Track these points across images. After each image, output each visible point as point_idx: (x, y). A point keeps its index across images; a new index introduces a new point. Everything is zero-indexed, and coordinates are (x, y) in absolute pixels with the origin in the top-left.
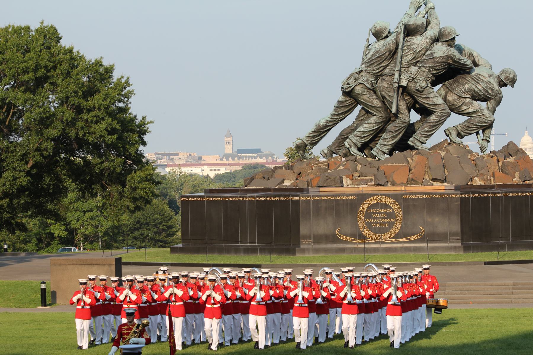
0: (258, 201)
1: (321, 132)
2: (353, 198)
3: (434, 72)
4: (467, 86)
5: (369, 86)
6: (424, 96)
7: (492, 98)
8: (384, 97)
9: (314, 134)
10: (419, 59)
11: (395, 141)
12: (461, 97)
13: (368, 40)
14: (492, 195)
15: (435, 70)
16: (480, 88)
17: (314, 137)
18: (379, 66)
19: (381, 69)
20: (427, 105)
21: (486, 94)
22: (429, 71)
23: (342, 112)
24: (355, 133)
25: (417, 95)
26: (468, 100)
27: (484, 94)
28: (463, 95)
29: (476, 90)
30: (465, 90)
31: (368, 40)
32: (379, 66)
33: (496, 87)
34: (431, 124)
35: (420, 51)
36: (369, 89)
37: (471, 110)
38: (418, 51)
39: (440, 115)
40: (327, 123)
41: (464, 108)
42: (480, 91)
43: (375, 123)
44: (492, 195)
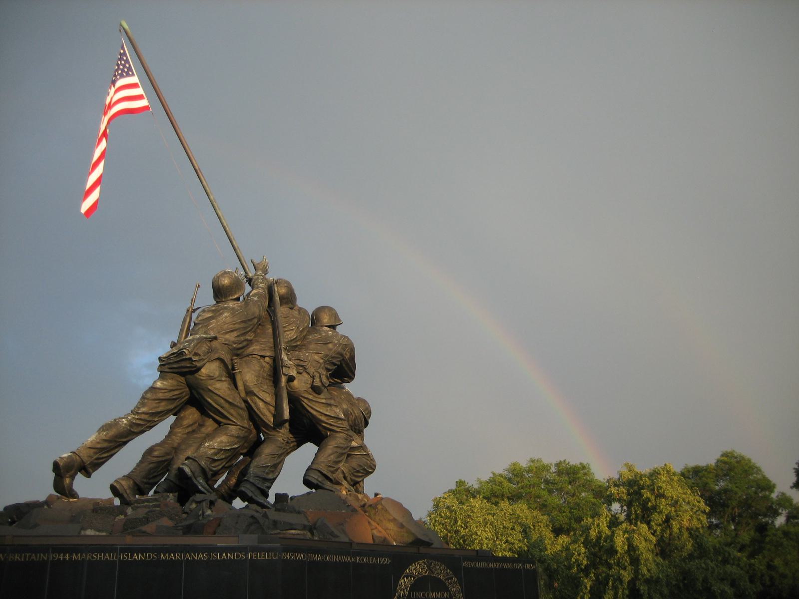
0: (123, 563)
1: (116, 440)
2: (386, 561)
5: (230, 367)
6: (324, 401)
8: (249, 393)
9: (105, 445)
10: (298, 343)
13: (193, 301)
17: (102, 450)
18: (242, 338)
19: (245, 343)
20: (323, 418)
22: (325, 362)
23: (160, 409)
25: (311, 397)
31: (193, 301)
32: (242, 338)
40: (131, 426)
43: (237, 437)
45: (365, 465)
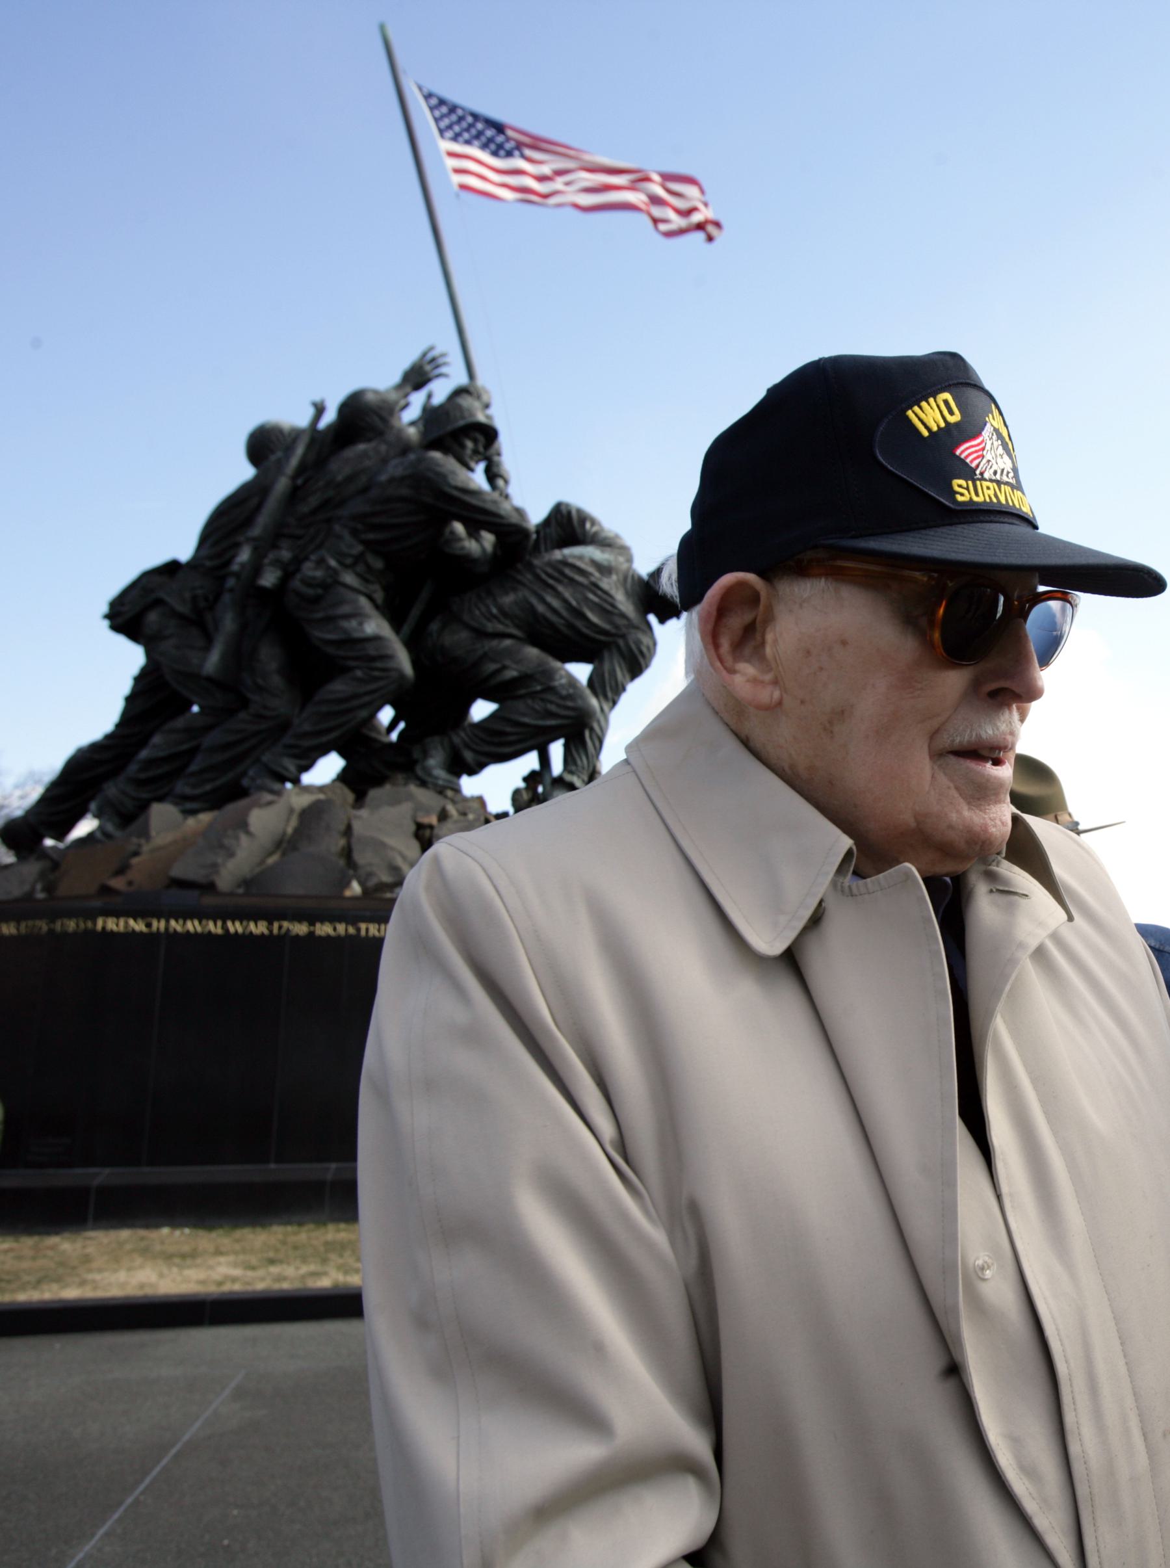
3: (371, 536)
4: (508, 600)
7: (606, 645)
11: (218, 783)
12: (481, 634)
14: (301, 929)
15: (374, 528)
16: (555, 603)
20: (331, 650)
21: (579, 624)
22: (354, 533)
24: (133, 768)
26: (508, 642)
27: (571, 626)
28: (490, 627)
29: (541, 608)
30: (501, 609)
33: (624, 603)
34: (324, 709)
35: (350, 479)
36: (181, 617)
37: (511, 674)
38: (340, 478)
39: (359, 673)
41: (492, 667)
42: (555, 611)
44: (301, 929)
45: (524, 715)
